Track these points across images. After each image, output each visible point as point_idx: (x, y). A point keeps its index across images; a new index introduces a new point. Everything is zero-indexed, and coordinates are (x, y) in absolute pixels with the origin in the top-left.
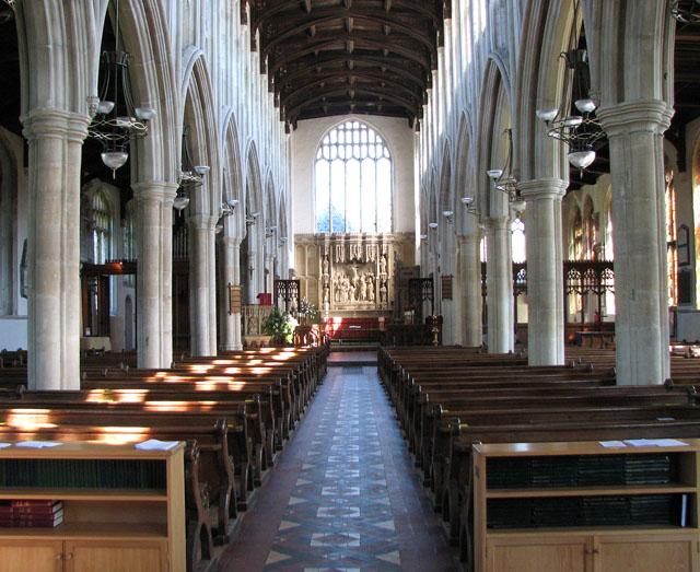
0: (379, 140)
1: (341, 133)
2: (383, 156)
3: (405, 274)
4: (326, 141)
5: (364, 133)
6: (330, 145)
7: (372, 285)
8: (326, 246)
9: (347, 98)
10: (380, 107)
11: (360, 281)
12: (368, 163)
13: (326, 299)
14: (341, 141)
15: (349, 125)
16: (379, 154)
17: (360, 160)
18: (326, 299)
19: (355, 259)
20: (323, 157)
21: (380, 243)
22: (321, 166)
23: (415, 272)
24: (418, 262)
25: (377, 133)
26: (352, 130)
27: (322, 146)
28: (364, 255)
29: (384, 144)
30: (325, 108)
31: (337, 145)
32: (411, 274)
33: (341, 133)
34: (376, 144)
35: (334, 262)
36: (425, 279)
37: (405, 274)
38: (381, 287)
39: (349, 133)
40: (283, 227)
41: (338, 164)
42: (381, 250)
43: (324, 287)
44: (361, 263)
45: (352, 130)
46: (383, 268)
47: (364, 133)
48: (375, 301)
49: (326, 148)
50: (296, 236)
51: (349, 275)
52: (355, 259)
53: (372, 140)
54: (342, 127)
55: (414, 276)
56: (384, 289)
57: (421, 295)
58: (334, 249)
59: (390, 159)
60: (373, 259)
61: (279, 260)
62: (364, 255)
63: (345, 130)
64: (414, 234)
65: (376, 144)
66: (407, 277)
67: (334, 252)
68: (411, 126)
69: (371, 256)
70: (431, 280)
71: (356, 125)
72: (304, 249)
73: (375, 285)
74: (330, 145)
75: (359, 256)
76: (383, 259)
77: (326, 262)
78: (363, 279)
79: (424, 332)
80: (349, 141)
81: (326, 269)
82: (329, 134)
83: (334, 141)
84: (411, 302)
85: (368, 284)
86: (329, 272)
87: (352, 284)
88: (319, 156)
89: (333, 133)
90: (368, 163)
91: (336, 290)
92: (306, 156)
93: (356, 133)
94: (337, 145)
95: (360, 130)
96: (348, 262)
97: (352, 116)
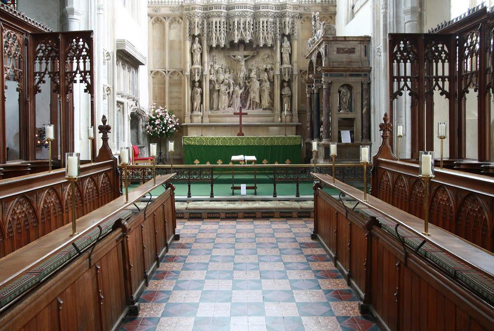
3: (339, 51)
7: (267, 84)
8: (197, 20)
11: (248, 78)
13: (197, 103)
19: (242, 42)
21: (282, 16)
28: (255, 33)
32: (352, 51)
35: (211, 49)
38: (282, 87)
42: (283, 26)
43: (193, 85)
44: (251, 47)
46: (286, 57)
48: (271, 107)
52: (242, 42)
56: (286, 91)
62: (255, 33)
67: (210, 32)
69: (265, 37)
72: (163, 24)
73: (272, 83)
75: (248, 38)
76: (286, 44)
77: (197, 46)
78: (253, 74)
81: (197, 57)
85: (261, 81)
86: (202, 63)
87: (236, 83)
91: (212, 91)
96: (232, 46)
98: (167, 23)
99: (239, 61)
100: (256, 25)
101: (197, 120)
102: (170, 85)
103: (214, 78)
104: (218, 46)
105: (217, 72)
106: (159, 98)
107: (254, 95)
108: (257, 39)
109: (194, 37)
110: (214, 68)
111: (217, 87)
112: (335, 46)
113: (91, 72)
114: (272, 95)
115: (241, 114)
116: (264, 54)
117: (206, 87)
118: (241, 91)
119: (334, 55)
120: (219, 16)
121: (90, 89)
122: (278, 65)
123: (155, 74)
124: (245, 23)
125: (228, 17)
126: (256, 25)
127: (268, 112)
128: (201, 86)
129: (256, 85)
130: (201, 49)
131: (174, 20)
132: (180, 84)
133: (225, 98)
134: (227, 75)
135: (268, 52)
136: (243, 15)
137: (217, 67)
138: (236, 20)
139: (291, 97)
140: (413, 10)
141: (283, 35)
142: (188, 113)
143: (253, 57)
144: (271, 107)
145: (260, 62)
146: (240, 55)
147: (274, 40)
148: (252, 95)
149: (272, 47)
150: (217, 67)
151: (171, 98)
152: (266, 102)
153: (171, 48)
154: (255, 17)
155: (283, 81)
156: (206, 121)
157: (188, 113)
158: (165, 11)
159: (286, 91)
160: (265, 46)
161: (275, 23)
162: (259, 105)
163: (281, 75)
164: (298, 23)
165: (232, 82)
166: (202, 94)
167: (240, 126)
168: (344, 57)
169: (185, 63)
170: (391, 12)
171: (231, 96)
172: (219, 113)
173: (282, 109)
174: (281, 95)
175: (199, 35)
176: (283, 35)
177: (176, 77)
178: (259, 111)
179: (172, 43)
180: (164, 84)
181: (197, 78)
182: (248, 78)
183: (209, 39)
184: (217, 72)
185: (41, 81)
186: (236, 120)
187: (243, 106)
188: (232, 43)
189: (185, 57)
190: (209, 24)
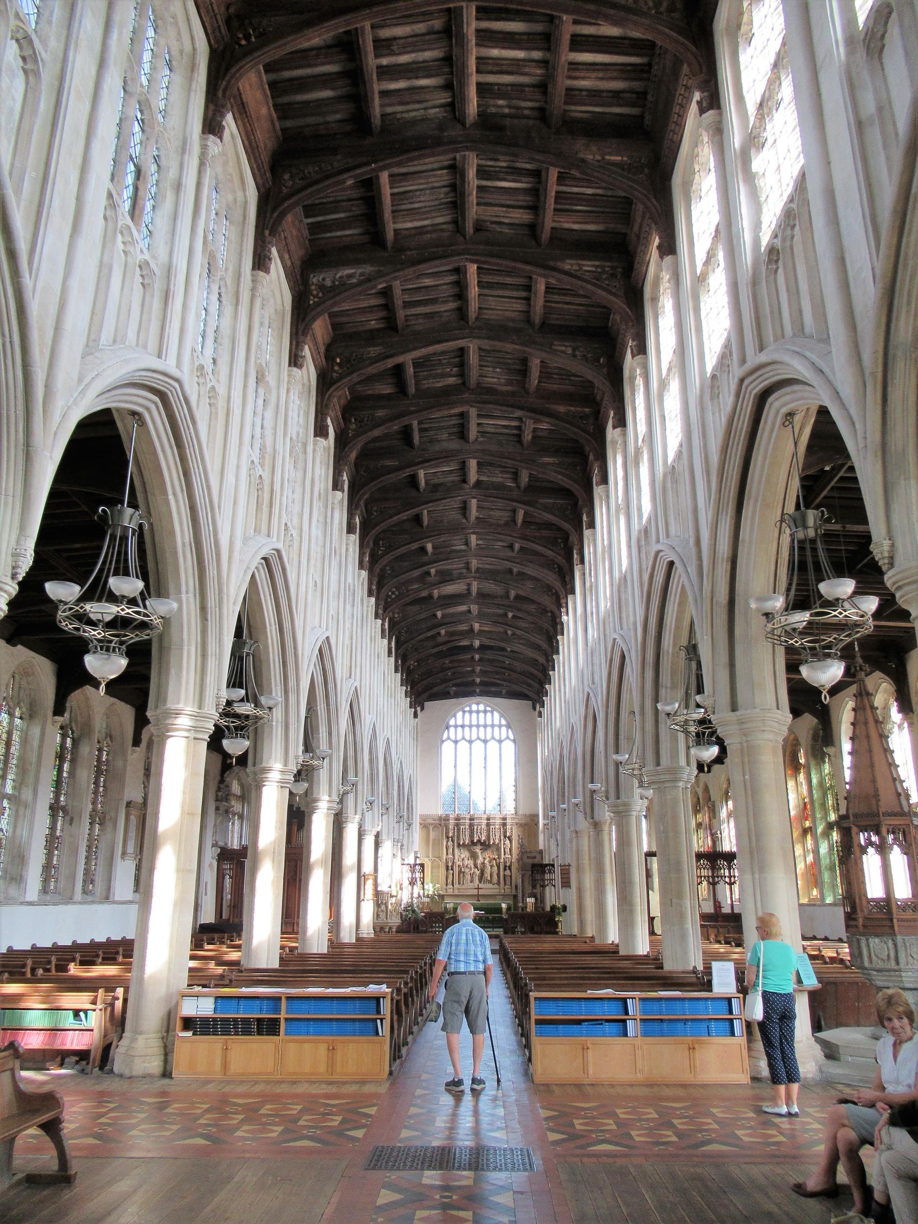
0: (504, 722)
1: (467, 715)
2: (508, 738)
4: (452, 722)
5: (489, 715)
6: (456, 726)
8: (451, 827)
9: (473, 683)
10: (504, 691)
11: (483, 863)
12: (493, 746)
13: (450, 880)
14: (467, 722)
15: (474, 707)
16: (504, 736)
17: (485, 741)
18: (450, 880)
19: (479, 841)
20: (449, 738)
21: (504, 825)
22: (447, 748)
23: (538, 856)
24: (541, 847)
25: (501, 716)
26: (478, 712)
27: (448, 727)
28: (488, 837)
29: (508, 726)
30: (452, 692)
31: (463, 726)
33: (467, 715)
34: (500, 726)
35: (459, 845)
36: (546, 865)
38: (505, 870)
39: (474, 715)
40: (410, 808)
41: (463, 745)
42: (505, 832)
43: (447, 869)
44: (485, 846)
45: (478, 712)
46: (508, 850)
47: (489, 715)
49: (452, 730)
51: (474, 856)
53: (496, 722)
54: (467, 709)
55: (536, 861)
57: (543, 880)
58: (459, 830)
59: (514, 741)
60: (497, 841)
61: (405, 843)
62: (488, 837)
63: (471, 712)
64: (538, 816)
65: (500, 726)
66: (531, 861)
68: (534, 708)
70: (553, 865)
71: (481, 707)
72: (429, 831)
74: (456, 726)
76: (508, 842)
77: (450, 843)
79: (545, 921)
80: (474, 722)
83: (459, 722)
84: (534, 887)
85: (492, 866)
86: (453, 854)
88: (445, 736)
89: (459, 715)
90: (493, 746)
91: (460, 872)
93: (482, 715)
94: (463, 726)
95: (485, 712)
97: (479, 699)
101: (450, 892)
115: (478, 889)
117: (456, 870)
126: (488, 831)
127: (496, 886)
128: (452, 869)
130: (453, 845)
144: (498, 883)
150: (463, 856)
155: (505, 866)
156: (456, 892)
158: (429, 821)
160: (494, 843)
162: (490, 882)
167: (478, 895)
171: (472, 875)
172: (464, 887)
174: (504, 876)
178: (490, 886)
181: (450, 864)
186: (475, 892)
187: (480, 882)
188: (472, 842)
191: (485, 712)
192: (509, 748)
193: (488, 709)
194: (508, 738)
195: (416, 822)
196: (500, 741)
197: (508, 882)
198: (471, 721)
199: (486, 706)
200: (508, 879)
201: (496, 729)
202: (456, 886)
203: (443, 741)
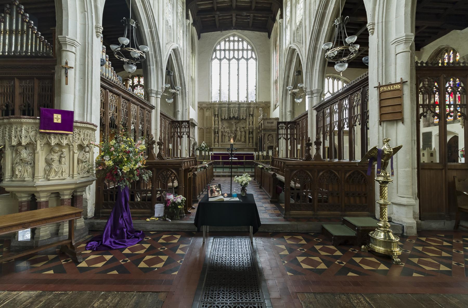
0: (249, 48)
1: (227, 43)
2: (252, 57)
4: (218, 48)
5: (241, 43)
7: (244, 133)
8: (217, 109)
11: (236, 130)
13: (216, 140)
15: (232, 38)
16: (249, 56)
17: (238, 60)
18: (216, 140)
19: (234, 117)
20: (216, 57)
22: (215, 63)
25: (248, 44)
26: (234, 41)
27: (215, 50)
29: (252, 50)
31: (225, 50)
33: (227, 43)
34: (247, 50)
35: (222, 119)
37: (268, 123)
38: (249, 134)
39: (232, 43)
43: (215, 133)
44: (238, 119)
47: (241, 43)
49: (218, 52)
50: (199, 103)
51: (230, 127)
52: (234, 117)
53: (245, 48)
56: (251, 135)
59: (256, 59)
60: (245, 117)
63: (229, 41)
69: (243, 116)
71: (236, 38)
73: (245, 132)
74: (220, 50)
76: (251, 118)
77: (216, 118)
78: (238, 129)
82: (220, 44)
83: (223, 48)
85: (241, 132)
86: (218, 125)
87: (231, 133)
89: (223, 43)
90: (243, 62)
91: (222, 135)
92: (204, 55)
94: (225, 50)
95: (238, 41)
97: (235, 32)
98: (205, 110)
99: (232, 124)
100: (239, 110)
101: (216, 146)
102: (206, 133)
103: (223, 131)
104: (225, 119)
105: (224, 128)
106: (202, 138)
107: (238, 137)
108: (240, 116)
109: (215, 115)
110: (223, 127)
111: (224, 134)
112: (266, 121)
113: (189, 132)
114: (245, 137)
116: (242, 121)
117: (220, 134)
118: (233, 135)
119: (266, 124)
120: (225, 107)
121: (189, 137)
122: (248, 126)
123: (200, 129)
124: (235, 110)
125: (229, 108)
126: (239, 110)
127: (244, 144)
128: (218, 133)
129: (239, 133)
131: (208, 109)
132: (210, 132)
133: (227, 138)
134: (228, 129)
135: (244, 121)
136: (234, 107)
137: (224, 126)
138: (232, 109)
139: (253, 138)
140: (290, 111)
141: (250, 115)
142: (213, 143)
143: (238, 122)
144: (245, 141)
145: (241, 125)
146: (233, 122)
147: (246, 116)
148: (238, 137)
149: (245, 119)
150: (224, 126)
151: (206, 138)
152: (243, 140)
153: (206, 119)
154: (239, 108)
155: (249, 132)
157: (213, 143)
158: (204, 105)
159: (251, 135)
160: (243, 119)
161: (246, 110)
163: (249, 129)
164: (255, 110)
165: (230, 132)
166: (218, 137)
168: (270, 125)
169: (212, 125)
170: (284, 111)
172: (225, 143)
173: (249, 142)
175: (217, 115)
176: (250, 115)
177: (208, 130)
179: (207, 117)
180: (204, 132)
182: (236, 130)
183: (221, 116)
184: (224, 128)
185: (183, 134)
188: (230, 117)
189: (212, 122)
190: (221, 110)
191: (238, 41)
192: (253, 64)
193: (240, 39)
194: (252, 57)
195: (196, 105)
196: (247, 60)
197: (251, 141)
198: (229, 47)
199: (239, 37)
200: (251, 139)
201: (245, 52)
202: (220, 143)
203: (212, 59)
